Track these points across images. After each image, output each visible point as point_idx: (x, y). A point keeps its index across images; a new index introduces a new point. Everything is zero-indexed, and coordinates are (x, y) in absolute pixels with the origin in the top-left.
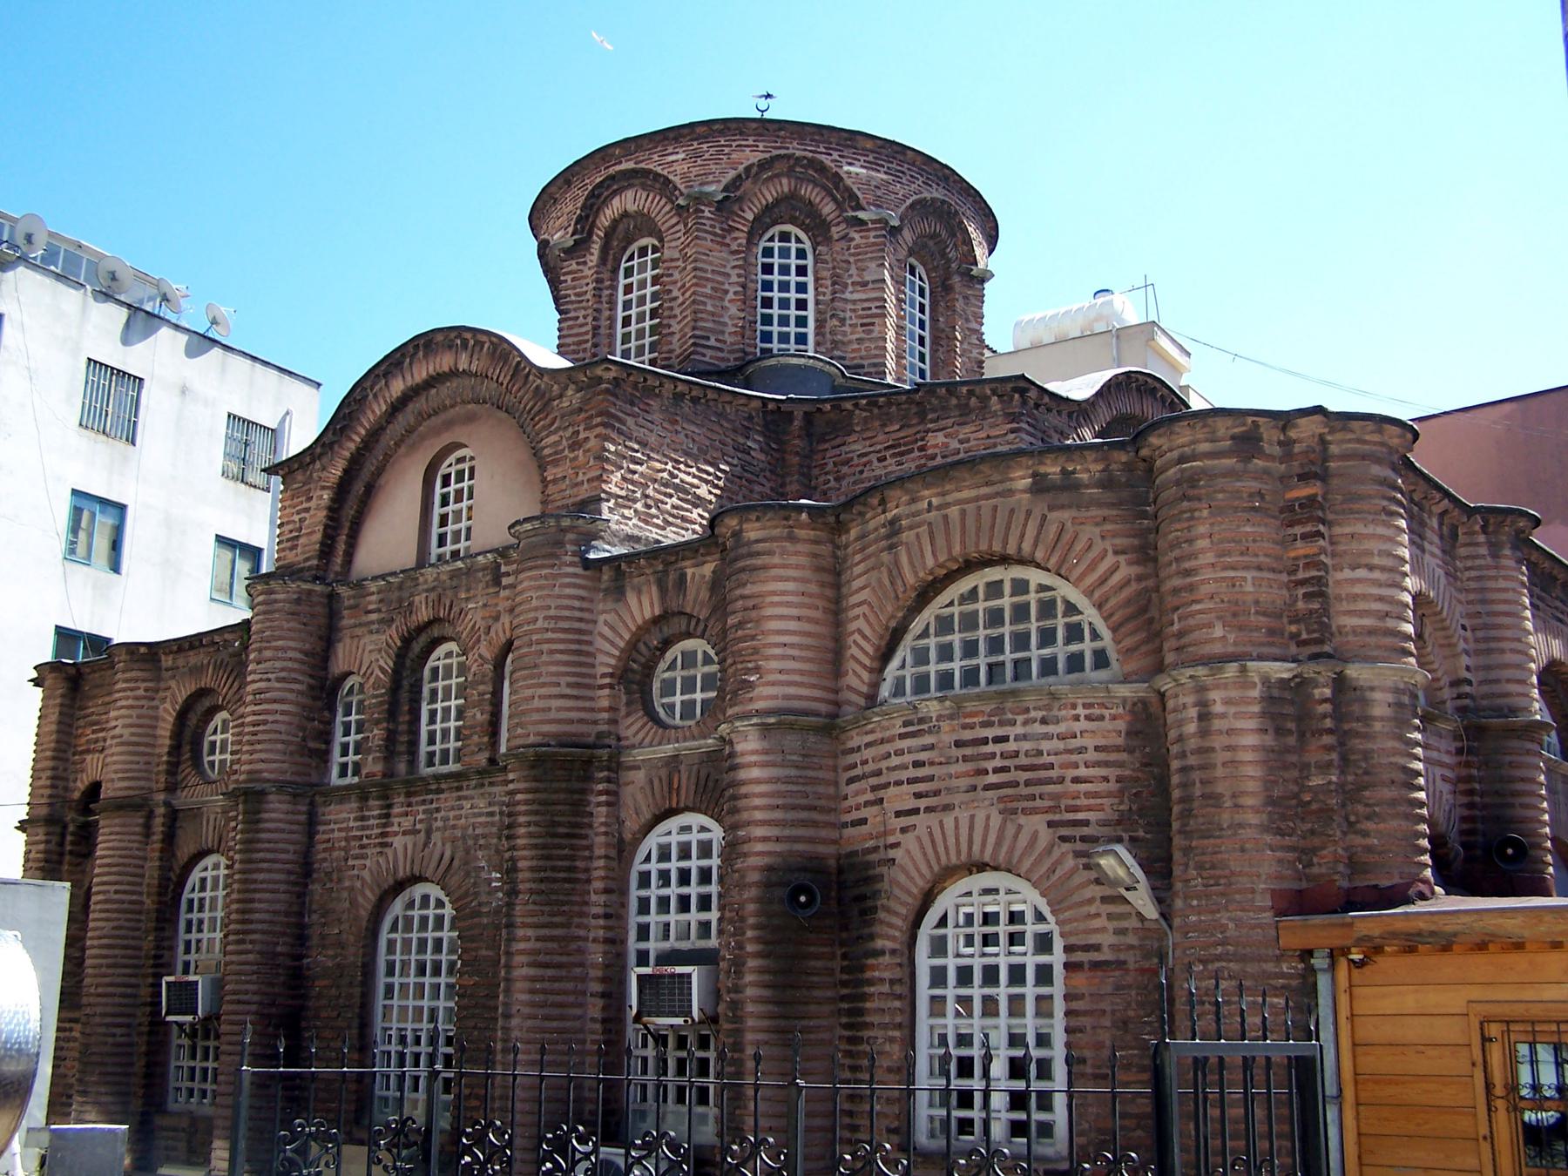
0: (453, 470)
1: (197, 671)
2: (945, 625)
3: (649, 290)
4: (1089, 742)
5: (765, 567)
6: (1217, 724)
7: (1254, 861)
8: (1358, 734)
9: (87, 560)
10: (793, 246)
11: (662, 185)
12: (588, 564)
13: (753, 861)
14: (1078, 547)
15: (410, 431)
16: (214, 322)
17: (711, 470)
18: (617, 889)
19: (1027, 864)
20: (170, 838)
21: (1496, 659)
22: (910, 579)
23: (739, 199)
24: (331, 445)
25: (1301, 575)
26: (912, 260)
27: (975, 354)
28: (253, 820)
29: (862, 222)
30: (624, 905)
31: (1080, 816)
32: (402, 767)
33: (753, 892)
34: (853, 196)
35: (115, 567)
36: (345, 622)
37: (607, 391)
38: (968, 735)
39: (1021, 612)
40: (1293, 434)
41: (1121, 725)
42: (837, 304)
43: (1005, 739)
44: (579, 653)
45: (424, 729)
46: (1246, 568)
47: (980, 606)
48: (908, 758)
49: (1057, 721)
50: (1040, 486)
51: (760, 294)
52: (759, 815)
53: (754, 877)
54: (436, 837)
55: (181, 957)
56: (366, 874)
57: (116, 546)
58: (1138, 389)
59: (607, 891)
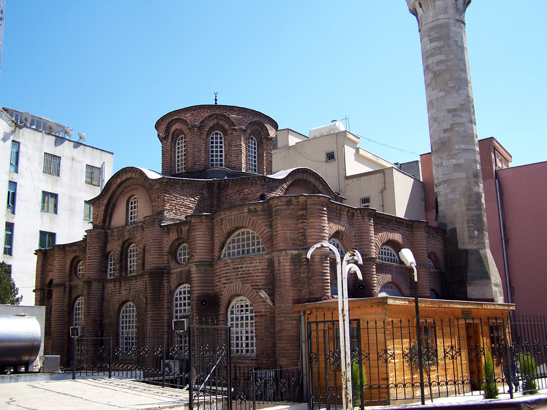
0: (133, 201)
1: (75, 251)
2: (233, 241)
3: (183, 149)
4: (259, 268)
5: (196, 229)
6: (282, 264)
7: (288, 293)
8: (311, 265)
9: (48, 211)
10: (219, 136)
11: (185, 122)
12: (161, 226)
13: (195, 295)
14: (257, 225)
15: (122, 191)
16: (81, 138)
17: (193, 200)
18: (170, 302)
19: (247, 294)
20: (70, 293)
21: (362, 243)
22: (225, 232)
23: (204, 126)
24: (104, 195)
25: (300, 231)
26: (252, 136)
27: (270, 159)
28: (89, 288)
29: (236, 129)
30: (172, 305)
31: (258, 284)
32: (124, 274)
33: (195, 302)
34: (233, 123)
35: (56, 212)
36: (109, 239)
37: (165, 185)
38: (235, 267)
39: (248, 239)
40: (299, 200)
41: (266, 264)
42: (230, 151)
43: (242, 267)
44: (159, 247)
45: (129, 264)
46: (288, 230)
47: (240, 237)
48: (225, 272)
49: (253, 263)
50: (250, 211)
51: (210, 149)
52: (196, 285)
53: (195, 298)
54: (131, 291)
55: (75, 322)
56: (116, 300)
57: (56, 206)
58: (302, 172)
59: (168, 302)
